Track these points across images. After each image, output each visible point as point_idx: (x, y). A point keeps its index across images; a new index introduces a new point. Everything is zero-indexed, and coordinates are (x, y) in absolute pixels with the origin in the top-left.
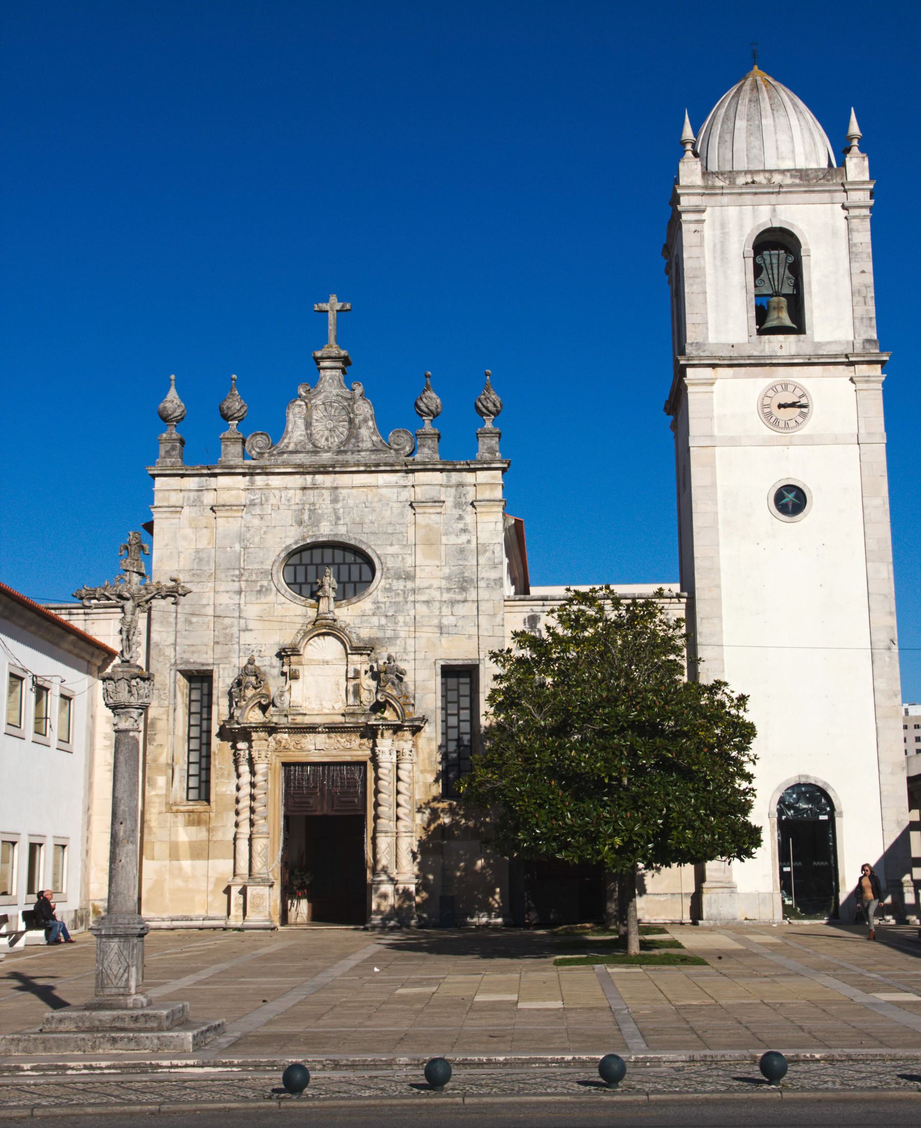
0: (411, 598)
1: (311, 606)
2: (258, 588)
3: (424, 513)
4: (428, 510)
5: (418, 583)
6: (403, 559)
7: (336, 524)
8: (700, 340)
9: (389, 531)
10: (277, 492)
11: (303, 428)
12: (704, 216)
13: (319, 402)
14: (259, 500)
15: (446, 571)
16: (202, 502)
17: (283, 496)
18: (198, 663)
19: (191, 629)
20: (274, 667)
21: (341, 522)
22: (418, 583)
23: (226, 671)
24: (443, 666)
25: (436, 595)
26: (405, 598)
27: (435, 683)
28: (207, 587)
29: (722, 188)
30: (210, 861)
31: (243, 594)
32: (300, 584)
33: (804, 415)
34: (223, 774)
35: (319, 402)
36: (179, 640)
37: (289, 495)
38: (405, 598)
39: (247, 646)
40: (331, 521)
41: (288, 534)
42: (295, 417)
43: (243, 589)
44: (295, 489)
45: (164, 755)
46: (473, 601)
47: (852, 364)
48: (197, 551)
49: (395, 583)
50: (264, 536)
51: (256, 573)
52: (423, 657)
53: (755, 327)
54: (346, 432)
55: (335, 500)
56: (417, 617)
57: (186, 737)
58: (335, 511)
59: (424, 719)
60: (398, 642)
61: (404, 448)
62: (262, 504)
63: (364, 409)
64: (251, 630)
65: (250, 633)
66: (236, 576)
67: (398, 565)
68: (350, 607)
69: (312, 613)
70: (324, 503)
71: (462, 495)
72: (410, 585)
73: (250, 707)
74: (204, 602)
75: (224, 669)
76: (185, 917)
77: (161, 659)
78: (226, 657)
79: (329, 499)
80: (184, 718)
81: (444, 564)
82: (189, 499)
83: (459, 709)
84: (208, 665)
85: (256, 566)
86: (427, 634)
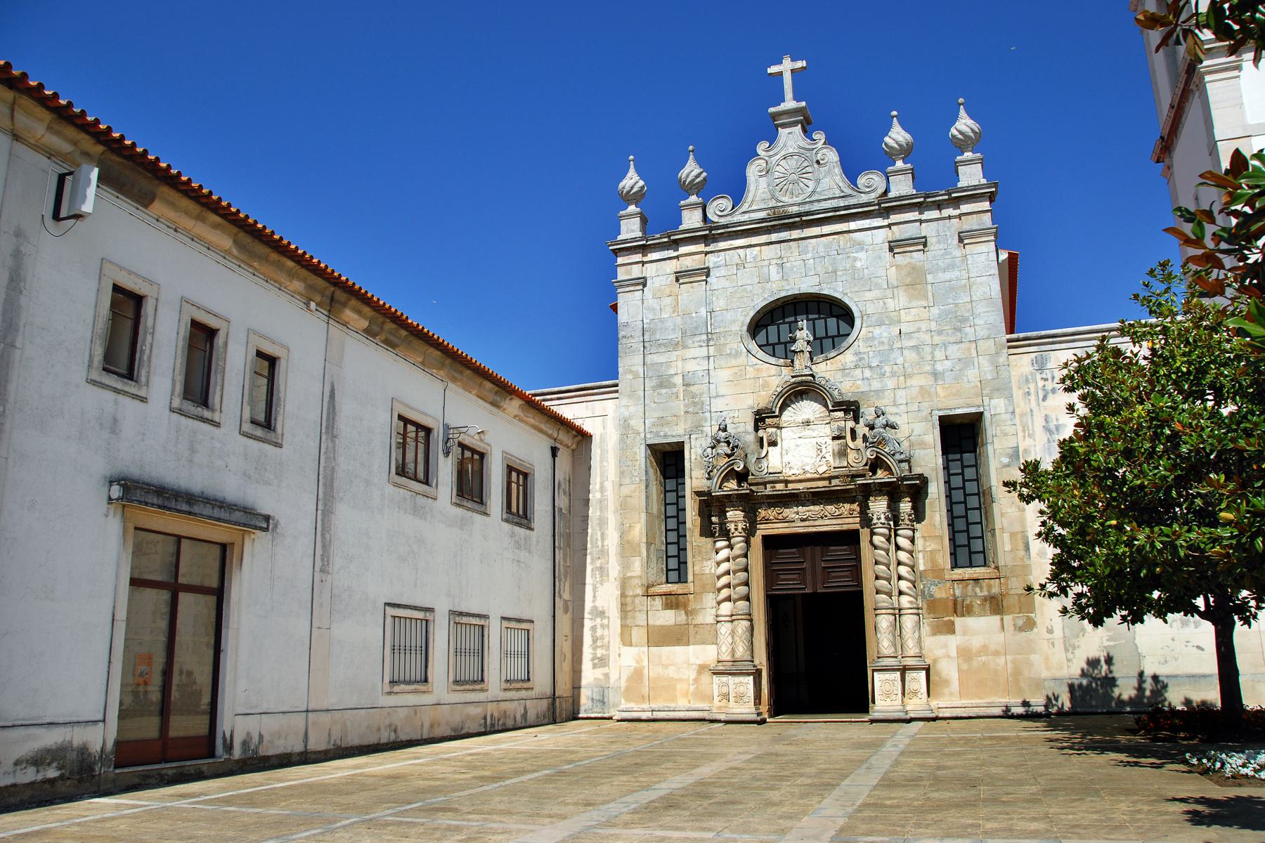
2: (728, 352)
3: (904, 252)
4: (908, 249)
6: (884, 303)
10: (741, 251)
15: (935, 311)
17: (748, 254)
20: (749, 433)
24: (942, 419)
25: (926, 338)
27: (933, 437)
30: (691, 647)
31: (712, 358)
32: (773, 345)
34: (700, 552)
37: (755, 253)
56: (906, 364)
57: (663, 517)
60: (887, 393)
66: (704, 341)
69: (786, 372)
74: (672, 371)
78: (698, 427)
80: (658, 495)
83: (963, 467)
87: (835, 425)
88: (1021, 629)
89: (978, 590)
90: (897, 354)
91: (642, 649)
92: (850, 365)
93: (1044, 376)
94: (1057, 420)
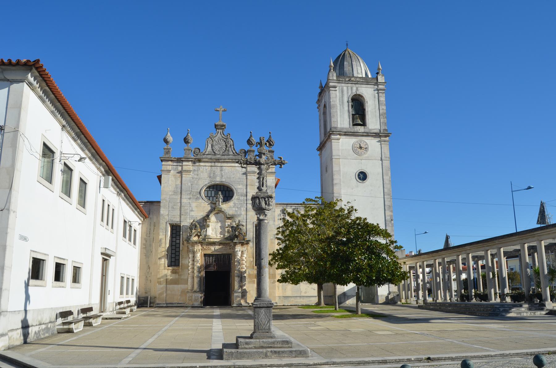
2: (196, 198)
4: (251, 175)
6: (243, 190)
8: (336, 126)
9: (239, 181)
12: (337, 89)
14: (197, 169)
20: (201, 223)
21: (224, 177)
29: (342, 81)
32: (209, 197)
33: (366, 151)
36: (169, 214)
37: (207, 168)
44: (208, 166)
47: (380, 137)
49: (241, 197)
51: (195, 193)
52: (249, 221)
53: (351, 124)
54: (225, 149)
55: (221, 170)
59: (249, 241)
60: (241, 216)
62: (198, 171)
64: (194, 211)
68: (226, 204)
77: (164, 219)
82: (173, 168)
85: (195, 190)
88: (272, 283)
93: (283, 215)
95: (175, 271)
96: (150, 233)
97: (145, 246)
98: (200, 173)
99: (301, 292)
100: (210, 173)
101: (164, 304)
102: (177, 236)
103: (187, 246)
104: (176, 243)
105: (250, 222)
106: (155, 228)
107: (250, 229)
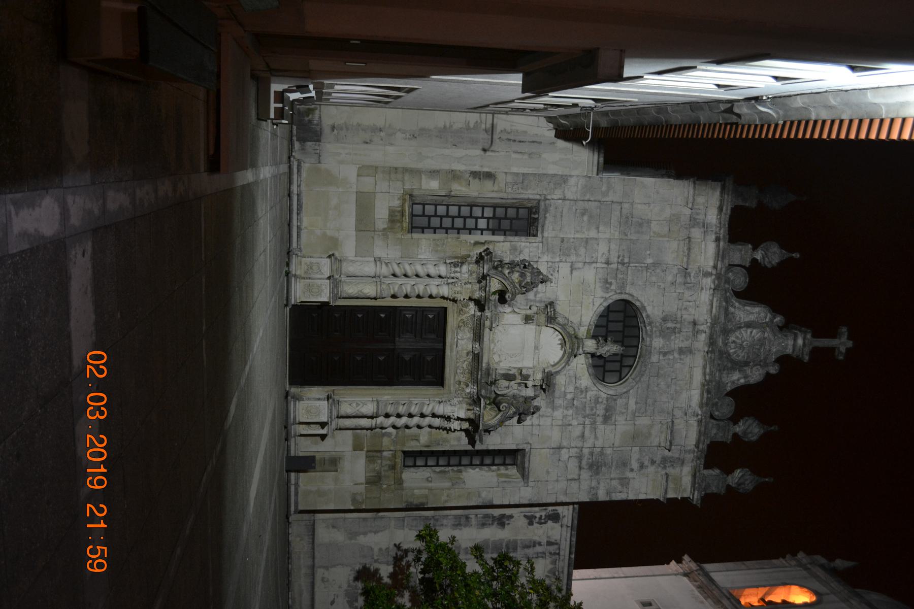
0: (587, 421)
1: (588, 330)
2: (609, 281)
3: (662, 432)
5: (601, 427)
6: (623, 413)
7: (660, 353)
9: (648, 401)
11: (746, 320)
13: (766, 335)
14: (689, 281)
15: (609, 451)
16: (693, 227)
17: (691, 303)
18: (544, 222)
19: (577, 215)
20: (535, 295)
21: (661, 358)
22: (601, 427)
23: (535, 249)
25: (589, 444)
26: (588, 416)
28: (616, 231)
30: (354, 233)
31: (606, 266)
32: (607, 316)
35: (766, 335)
37: (690, 309)
38: (588, 416)
39: (557, 270)
40: (663, 347)
41: (656, 308)
42: (756, 313)
43: (609, 266)
45: (459, 188)
46: (580, 475)
48: (649, 222)
50: (656, 285)
51: (623, 278)
52: (533, 433)
55: (681, 351)
56: (571, 427)
58: (671, 352)
60: (550, 410)
61: (717, 410)
63: (755, 375)
64: (572, 273)
65: (569, 272)
66: (622, 260)
67: (618, 408)
69: (582, 332)
70: (677, 342)
71: (672, 463)
72: (600, 420)
73: (503, 281)
74: (601, 228)
75: (538, 247)
76: (301, 207)
77: (552, 185)
79: (683, 346)
81: (615, 449)
82: (698, 214)
84: (542, 232)
85: (630, 278)
86: (555, 436)
87: (530, 372)
89: (386, 468)
90: (581, 420)
91: (355, 186)
92: (579, 382)
93: (543, 518)
94: (509, 524)
95: (398, 218)
96: (509, 140)
97: (472, 125)
98: (677, 291)
99: (327, 568)
100: (675, 321)
101: (299, 186)
102: (496, 221)
103: (471, 254)
104: (477, 218)
105: (532, 434)
106: (526, 157)
107: (512, 433)
